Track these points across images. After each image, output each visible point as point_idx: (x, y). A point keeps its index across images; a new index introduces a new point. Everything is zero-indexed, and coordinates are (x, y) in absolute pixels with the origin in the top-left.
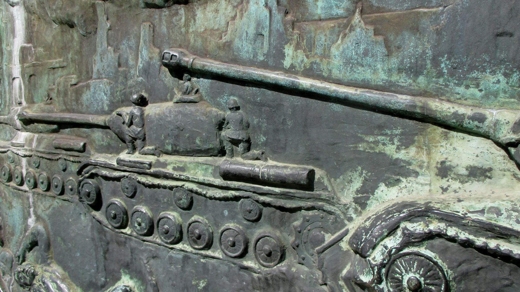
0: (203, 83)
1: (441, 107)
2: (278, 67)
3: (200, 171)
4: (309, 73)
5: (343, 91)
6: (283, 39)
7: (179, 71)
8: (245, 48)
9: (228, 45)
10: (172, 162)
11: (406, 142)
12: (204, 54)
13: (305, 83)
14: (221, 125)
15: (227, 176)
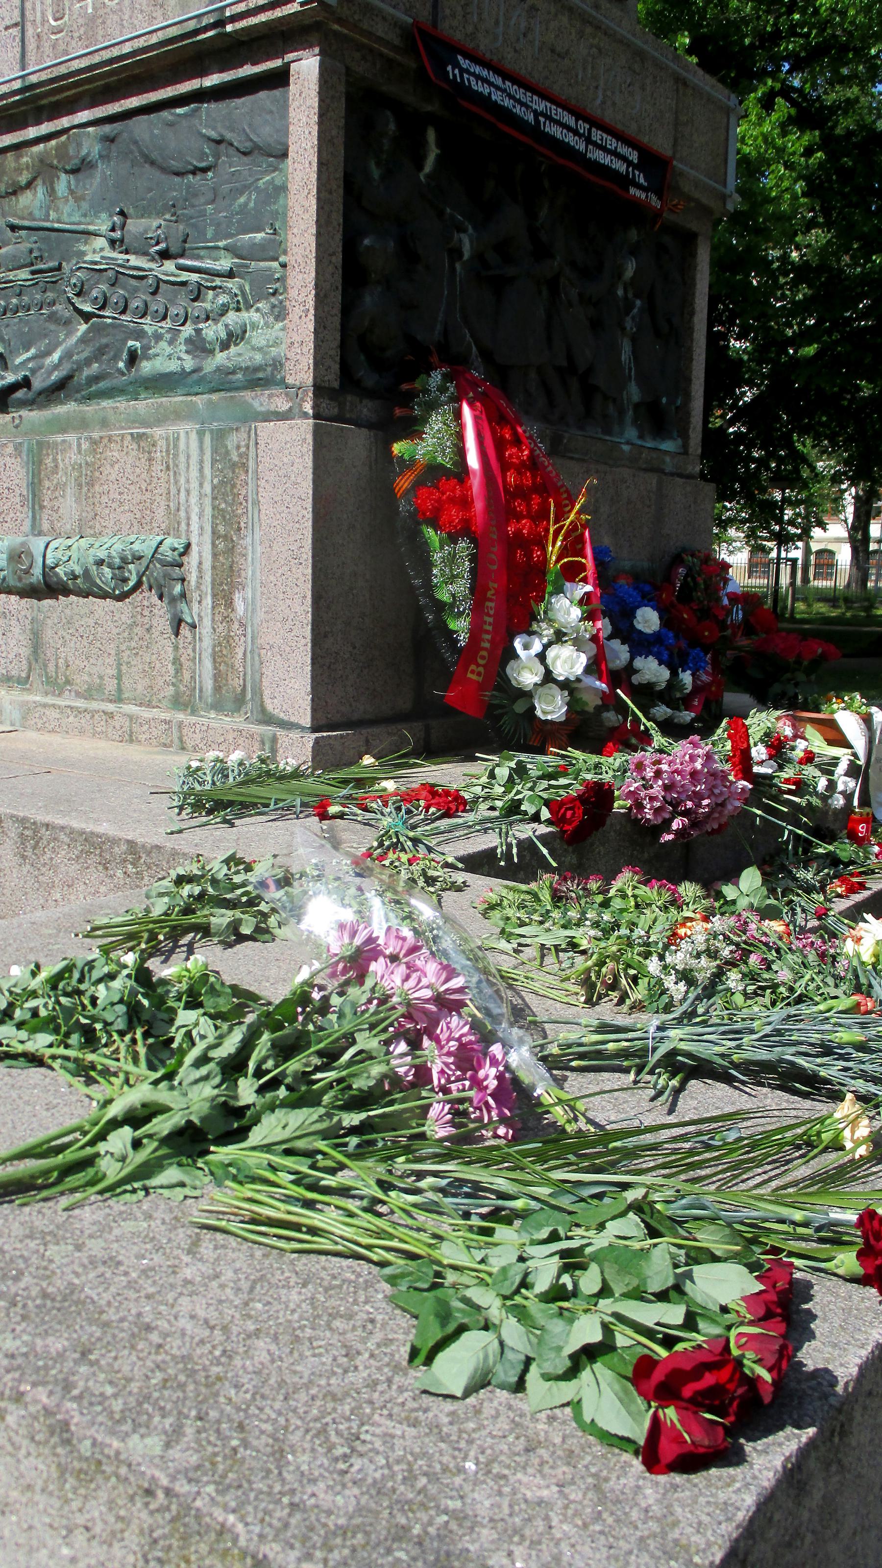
0: (23, 233)
1: (91, 228)
2: (47, 220)
3: (24, 274)
4: (59, 222)
5: (67, 227)
6: (48, 208)
7: (13, 228)
8: (37, 214)
9: (31, 214)
10: (11, 275)
11: (86, 243)
12: (23, 218)
13: (56, 225)
14: (31, 251)
15: (33, 273)
